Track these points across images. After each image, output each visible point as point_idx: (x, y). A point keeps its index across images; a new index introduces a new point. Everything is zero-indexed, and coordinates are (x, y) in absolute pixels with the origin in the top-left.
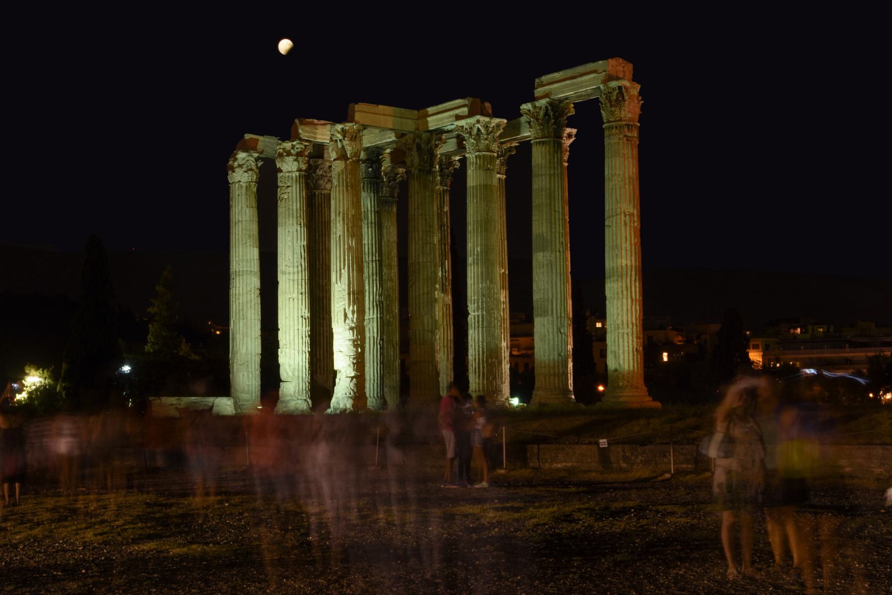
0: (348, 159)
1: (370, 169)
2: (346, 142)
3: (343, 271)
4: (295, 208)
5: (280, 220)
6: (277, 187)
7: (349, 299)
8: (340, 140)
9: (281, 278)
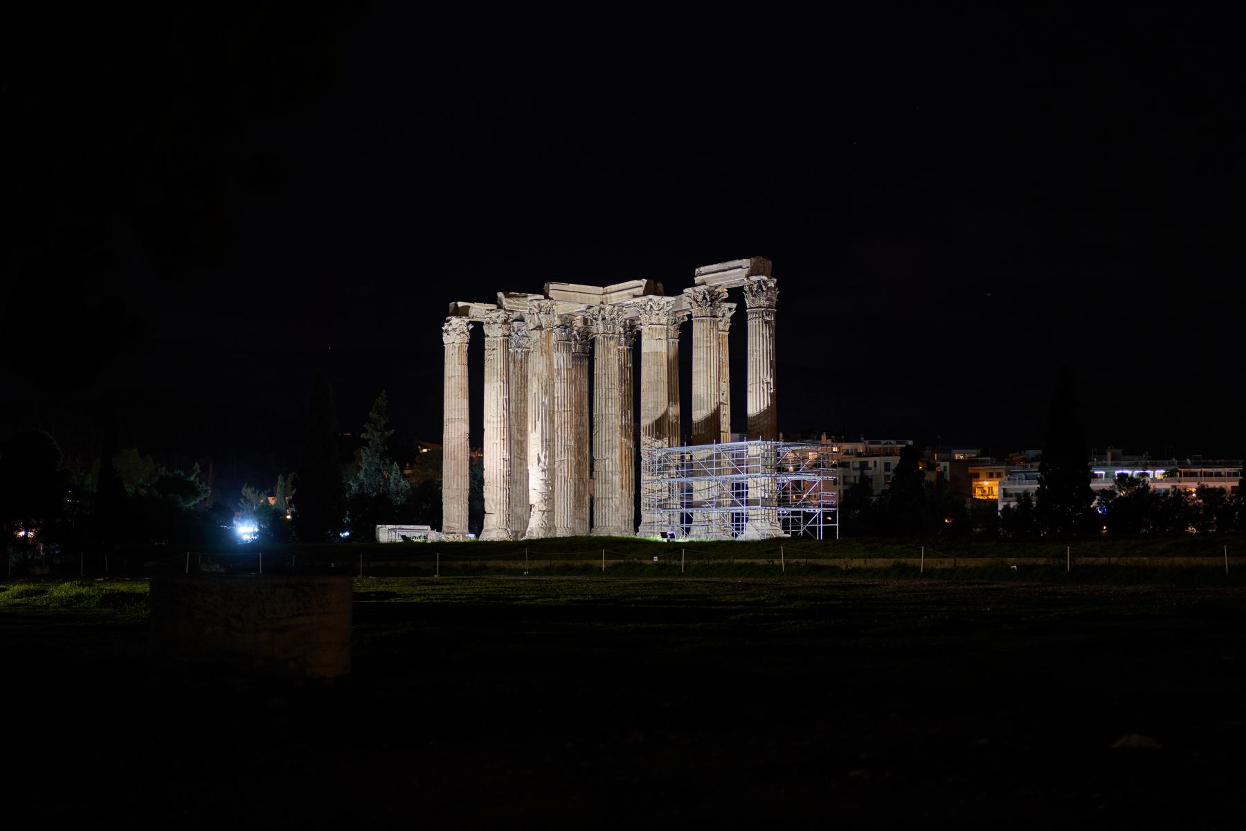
0: (543, 329)
1: (563, 333)
2: (541, 315)
3: (537, 422)
4: (499, 367)
5: (486, 377)
6: (484, 349)
7: (542, 446)
8: (537, 313)
9: (486, 426)
